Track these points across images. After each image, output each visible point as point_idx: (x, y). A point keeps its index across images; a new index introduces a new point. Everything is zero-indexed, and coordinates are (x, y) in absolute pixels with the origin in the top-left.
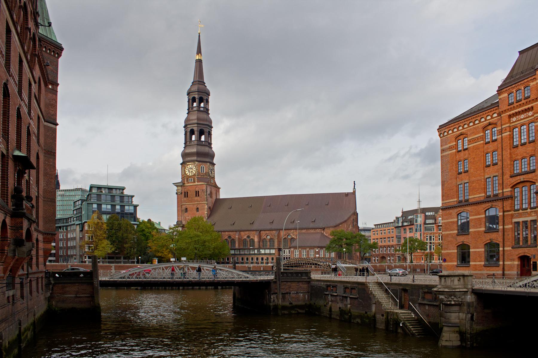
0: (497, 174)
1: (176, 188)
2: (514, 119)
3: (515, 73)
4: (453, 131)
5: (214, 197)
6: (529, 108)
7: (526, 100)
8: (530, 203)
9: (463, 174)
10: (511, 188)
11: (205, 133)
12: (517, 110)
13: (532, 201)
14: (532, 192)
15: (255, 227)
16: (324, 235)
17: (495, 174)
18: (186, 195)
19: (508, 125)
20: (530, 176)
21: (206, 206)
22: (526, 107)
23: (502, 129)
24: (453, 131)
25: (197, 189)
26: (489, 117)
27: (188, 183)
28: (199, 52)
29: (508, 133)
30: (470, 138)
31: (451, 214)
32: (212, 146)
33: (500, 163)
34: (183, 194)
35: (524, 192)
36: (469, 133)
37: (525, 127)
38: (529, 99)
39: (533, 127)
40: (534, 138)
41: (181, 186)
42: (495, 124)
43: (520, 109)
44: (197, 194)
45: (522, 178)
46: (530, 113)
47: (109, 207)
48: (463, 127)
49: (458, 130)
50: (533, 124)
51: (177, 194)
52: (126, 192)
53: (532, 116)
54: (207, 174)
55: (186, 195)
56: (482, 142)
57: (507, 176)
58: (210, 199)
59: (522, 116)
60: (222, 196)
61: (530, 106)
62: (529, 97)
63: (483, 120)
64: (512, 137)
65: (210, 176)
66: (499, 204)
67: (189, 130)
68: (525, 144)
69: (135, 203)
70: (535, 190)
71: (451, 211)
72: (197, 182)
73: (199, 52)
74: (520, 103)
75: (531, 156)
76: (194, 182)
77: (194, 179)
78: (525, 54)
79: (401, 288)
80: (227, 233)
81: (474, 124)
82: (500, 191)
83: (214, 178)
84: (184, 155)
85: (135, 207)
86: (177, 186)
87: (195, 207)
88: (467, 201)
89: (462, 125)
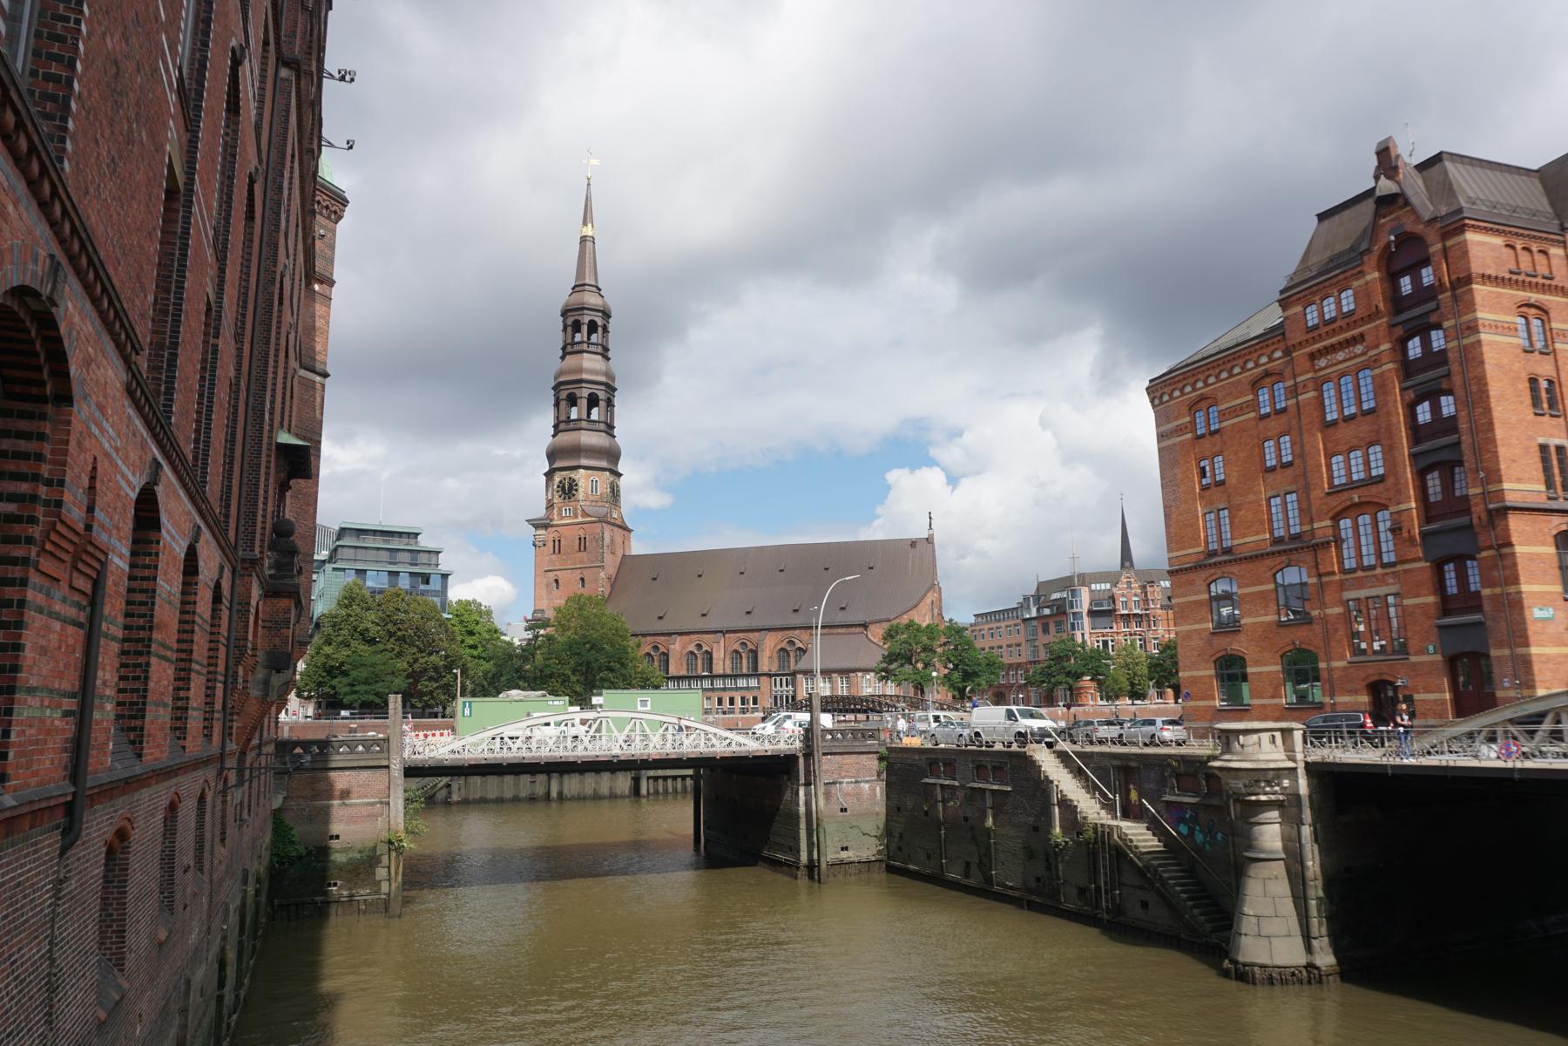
0: (1294, 487)
2: (1322, 363)
4: (1182, 390)
6: (1354, 338)
8: (1379, 554)
9: (1214, 489)
13: (1384, 549)
19: (1310, 375)
20: (1374, 490)
22: (1348, 335)
23: (1296, 385)
24: (1182, 390)
25: (582, 534)
26: (1264, 360)
29: (1313, 394)
30: (1222, 407)
31: (1192, 583)
32: (616, 432)
35: (1361, 529)
36: (1220, 395)
37: (1349, 378)
39: (1369, 380)
40: (1372, 404)
42: (1278, 375)
43: (1334, 340)
46: (1359, 349)
47: (385, 578)
49: (1194, 389)
50: (1368, 372)
53: (1364, 354)
55: (557, 547)
56: (1252, 415)
57: (1316, 494)
59: (1341, 356)
60: (637, 548)
61: (1355, 332)
62: (1351, 313)
63: (1250, 365)
67: (563, 395)
68: (1352, 417)
69: (443, 568)
70: (1388, 524)
71: (1192, 576)
74: (1335, 326)
81: (1231, 375)
84: (552, 455)
86: (536, 527)
88: (1228, 551)
89: (1202, 377)
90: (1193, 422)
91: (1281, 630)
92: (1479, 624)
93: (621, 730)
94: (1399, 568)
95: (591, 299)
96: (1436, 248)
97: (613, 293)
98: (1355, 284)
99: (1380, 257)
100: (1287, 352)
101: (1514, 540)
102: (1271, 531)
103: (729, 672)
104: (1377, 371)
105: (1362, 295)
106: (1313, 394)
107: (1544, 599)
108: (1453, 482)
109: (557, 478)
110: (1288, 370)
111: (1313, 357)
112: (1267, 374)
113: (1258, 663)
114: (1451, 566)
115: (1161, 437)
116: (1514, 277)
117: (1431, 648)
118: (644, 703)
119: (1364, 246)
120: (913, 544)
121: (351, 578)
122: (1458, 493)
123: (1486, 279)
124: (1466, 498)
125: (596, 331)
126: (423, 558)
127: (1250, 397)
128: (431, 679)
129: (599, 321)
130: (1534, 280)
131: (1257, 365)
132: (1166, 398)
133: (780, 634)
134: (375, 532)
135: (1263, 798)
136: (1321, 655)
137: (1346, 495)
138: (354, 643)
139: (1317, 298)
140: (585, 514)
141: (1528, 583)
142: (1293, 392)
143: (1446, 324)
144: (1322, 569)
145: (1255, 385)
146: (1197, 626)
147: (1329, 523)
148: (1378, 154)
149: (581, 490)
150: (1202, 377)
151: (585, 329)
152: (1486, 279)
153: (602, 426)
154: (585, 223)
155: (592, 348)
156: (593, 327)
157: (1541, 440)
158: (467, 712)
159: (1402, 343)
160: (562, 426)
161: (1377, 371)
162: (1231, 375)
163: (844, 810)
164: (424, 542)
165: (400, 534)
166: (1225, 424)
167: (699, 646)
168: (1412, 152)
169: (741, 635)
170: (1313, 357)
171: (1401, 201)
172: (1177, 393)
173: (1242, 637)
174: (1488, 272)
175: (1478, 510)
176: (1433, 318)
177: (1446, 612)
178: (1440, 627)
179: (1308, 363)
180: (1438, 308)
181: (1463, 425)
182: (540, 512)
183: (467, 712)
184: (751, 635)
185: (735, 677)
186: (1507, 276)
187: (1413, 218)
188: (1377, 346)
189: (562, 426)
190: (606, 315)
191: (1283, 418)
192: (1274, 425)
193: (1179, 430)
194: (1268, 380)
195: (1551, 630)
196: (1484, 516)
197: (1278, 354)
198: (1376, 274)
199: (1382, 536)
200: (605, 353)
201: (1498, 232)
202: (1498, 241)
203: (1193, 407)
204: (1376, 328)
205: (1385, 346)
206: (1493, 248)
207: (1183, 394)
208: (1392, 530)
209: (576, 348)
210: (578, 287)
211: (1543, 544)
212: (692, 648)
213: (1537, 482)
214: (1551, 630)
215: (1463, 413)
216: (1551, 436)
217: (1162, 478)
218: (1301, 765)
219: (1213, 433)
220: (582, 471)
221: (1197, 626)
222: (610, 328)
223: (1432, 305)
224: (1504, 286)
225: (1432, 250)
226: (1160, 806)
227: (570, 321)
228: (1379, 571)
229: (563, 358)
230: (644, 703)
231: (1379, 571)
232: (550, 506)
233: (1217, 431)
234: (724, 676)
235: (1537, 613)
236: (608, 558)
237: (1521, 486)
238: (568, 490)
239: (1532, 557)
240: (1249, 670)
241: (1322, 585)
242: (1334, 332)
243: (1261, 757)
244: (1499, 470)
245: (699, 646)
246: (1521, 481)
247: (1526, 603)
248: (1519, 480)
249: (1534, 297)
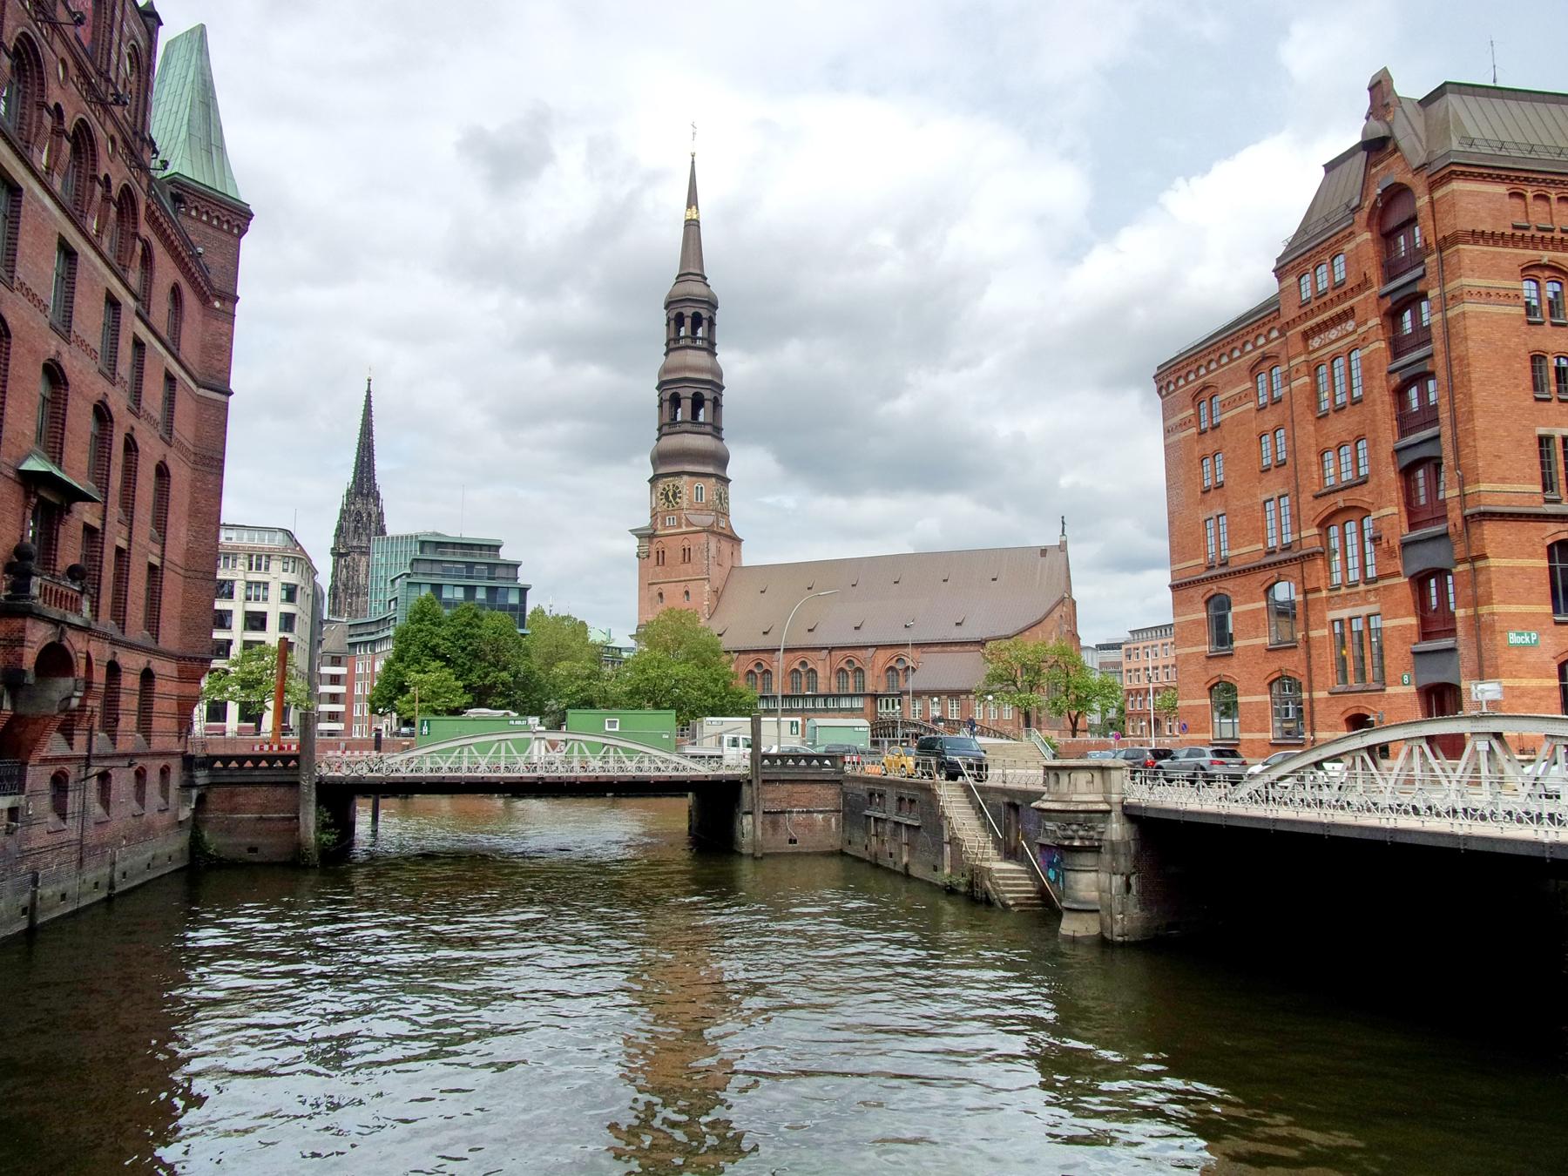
2: (1315, 343)
3: (1315, 218)
5: (728, 565)
7: (1337, 292)
10: (1319, 526)
12: (1318, 319)
14: (1367, 536)
17: (1282, 491)
18: (661, 558)
22: (1338, 309)
25: (686, 544)
27: (666, 528)
28: (692, 200)
32: (724, 434)
33: (1290, 461)
34: (654, 556)
38: (1344, 289)
43: (1325, 316)
44: (686, 554)
45: (1340, 500)
46: (1350, 325)
47: (460, 594)
48: (1207, 368)
53: (1354, 331)
55: (661, 558)
57: (1306, 497)
58: (715, 570)
59: (1333, 334)
60: (750, 556)
61: (1346, 306)
62: (1343, 283)
64: (1315, 392)
66: (1294, 570)
67: (667, 395)
69: (522, 581)
71: (1191, 592)
73: (692, 200)
75: (1359, 439)
76: (680, 526)
77: (679, 518)
78: (1337, 171)
79: (1006, 799)
82: (1296, 537)
84: (660, 458)
85: (523, 591)
86: (640, 537)
87: (681, 588)
90: (1198, 415)
91: (1270, 655)
92: (1452, 650)
93: (521, 752)
94: (1381, 584)
95: (695, 289)
96: (1422, 201)
97: (719, 280)
98: (1347, 247)
99: (1370, 218)
100: (1282, 334)
101: (1488, 552)
102: (1266, 544)
103: (835, 691)
104: (1366, 351)
105: (1353, 261)
106: (1307, 379)
107: (1525, 623)
108: (1438, 483)
109: (661, 485)
110: (1283, 356)
111: (1306, 336)
112: (1265, 358)
113: (1247, 692)
114: (1433, 582)
115: (1168, 432)
116: (1519, 233)
117: (1406, 679)
118: (612, 724)
119: (1355, 202)
120: (1044, 552)
121: (426, 591)
122: (1441, 497)
123: (1477, 236)
124: (1444, 503)
125: (700, 324)
126: (500, 572)
127: (1249, 385)
128: (501, 694)
129: (705, 314)
130: (1548, 235)
131: (1255, 348)
132: (1172, 387)
133: (890, 652)
134: (454, 545)
135: (1077, 843)
136: (1305, 684)
137: (1332, 499)
138: (424, 659)
139: (1310, 266)
140: (689, 524)
141: (1503, 602)
142: (1287, 378)
143: (1431, 294)
144: (1308, 587)
145: (1254, 370)
146: (1195, 649)
147: (1315, 531)
148: (1371, 89)
149: (685, 498)
150: (1204, 363)
151: (688, 321)
152: (1477, 236)
153: (708, 429)
154: (689, 207)
155: (699, 343)
156: (697, 320)
157: (1542, 431)
158: (425, 730)
159: (1394, 315)
160: (666, 429)
161: (1366, 351)
162: (1231, 360)
163: (793, 841)
164: (505, 555)
165: (481, 547)
166: (1225, 416)
167: (804, 664)
168: (1411, 86)
169: (848, 653)
170: (1306, 336)
171: (1391, 147)
172: (1182, 382)
173: (1234, 661)
174: (1480, 228)
175: (1455, 515)
176: (1420, 287)
177: (1426, 636)
178: (1415, 653)
179: (1301, 345)
180: (1424, 275)
181: (1444, 415)
182: (644, 521)
183: (425, 730)
184: (858, 653)
185: (839, 696)
186: (1509, 231)
187: (1402, 165)
188: (1365, 322)
190: (713, 305)
191: (1279, 408)
192: (1270, 419)
193: (1184, 424)
194: (1266, 364)
195: (1531, 658)
196: (1459, 522)
197: (1275, 334)
198: (1367, 235)
199: (1368, 544)
200: (711, 349)
201: (1500, 179)
202: (1502, 189)
203: (1196, 398)
204: (1366, 299)
205: (1375, 321)
206: (1491, 198)
207: (1187, 383)
208: (1373, 540)
209: (682, 343)
210: (682, 277)
211: (1531, 556)
212: (796, 665)
213: (1531, 481)
214: (1531, 658)
215: (1445, 400)
216: (1558, 425)
217: (1168, 480)
218: (1118, 808)
219: (1215, 427)
220: (685, 478)
221: (1195, 649)
222: (717, 320)
223: (1418, 271)
224: (1505, 245)
225: (1419, 204)
226: (1037, 849)
227: (673, 314)
228: (1362, 587)
229: (666, 354)
230: (612, 724)
231: (1344, 590)
232: (654, 516)
233: (1218, 425)
234: (826, 697)
235: (1513, 638)
236: (715, 570)
237: (1507, 487)
238: (671, 497)
239: (1512, 572)
240: (1240, 699)
241: (1306, 603)
242: (1326, 306)
243: (1075, 798)
244: (1476, 468)
246: (1508, 480)
247: (1498, 626)
248: (1503, 480)
249: (1546, 256)
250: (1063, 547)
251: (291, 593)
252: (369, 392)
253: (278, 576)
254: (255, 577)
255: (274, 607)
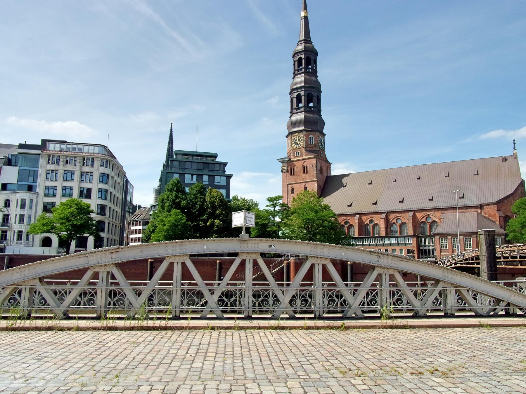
1: (281, 165)
5: (325, 174)
11: (313, 100)
15: (379, 208)
16: (482, 216)
21: (316, 185)
32: (322, 113)
41: (287, 162)
44: (305, 170)
51: (282, 171)
52: (218, 160)
54: (316, 145)
65: (319, 148)
69: (228, 173)
72: (305, 156)
76: (302, 156)
77: (302, 152)
80: (343, 218)
83: (324, 151)
85: (229, 177)
86: (282, 162)
189: (294, 111)
245: (371, 221)
250: (515, 156)
251: (105, 178)
252: (171, 128)
253: (98, 169)
254: (86, 169)
255: (95, 186)
